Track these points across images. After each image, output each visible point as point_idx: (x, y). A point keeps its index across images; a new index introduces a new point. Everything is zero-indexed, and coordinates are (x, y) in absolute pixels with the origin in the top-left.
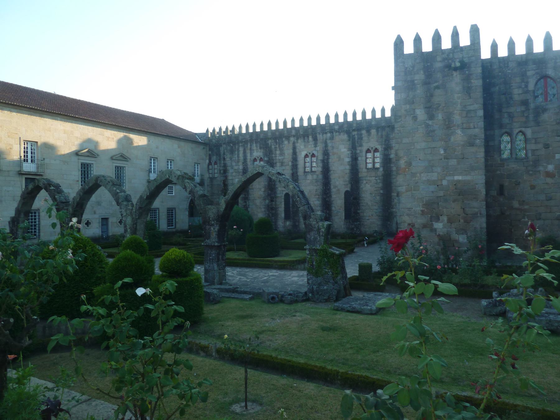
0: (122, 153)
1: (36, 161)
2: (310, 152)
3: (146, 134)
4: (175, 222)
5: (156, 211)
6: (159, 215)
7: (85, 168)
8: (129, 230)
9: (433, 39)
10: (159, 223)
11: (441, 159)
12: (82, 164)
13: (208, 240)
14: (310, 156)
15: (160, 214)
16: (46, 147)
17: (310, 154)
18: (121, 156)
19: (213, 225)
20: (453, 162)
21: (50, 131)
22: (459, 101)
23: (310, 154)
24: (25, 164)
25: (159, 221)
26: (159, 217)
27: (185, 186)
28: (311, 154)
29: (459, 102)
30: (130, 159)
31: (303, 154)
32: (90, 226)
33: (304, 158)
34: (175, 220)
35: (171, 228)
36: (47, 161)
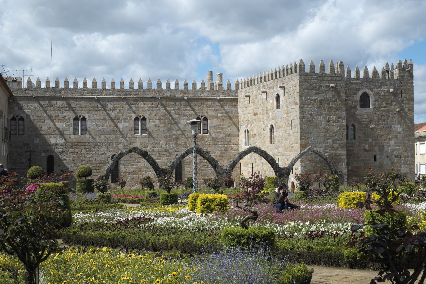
2: (140, 115)
3: (7, 89)
20: (331, 141)
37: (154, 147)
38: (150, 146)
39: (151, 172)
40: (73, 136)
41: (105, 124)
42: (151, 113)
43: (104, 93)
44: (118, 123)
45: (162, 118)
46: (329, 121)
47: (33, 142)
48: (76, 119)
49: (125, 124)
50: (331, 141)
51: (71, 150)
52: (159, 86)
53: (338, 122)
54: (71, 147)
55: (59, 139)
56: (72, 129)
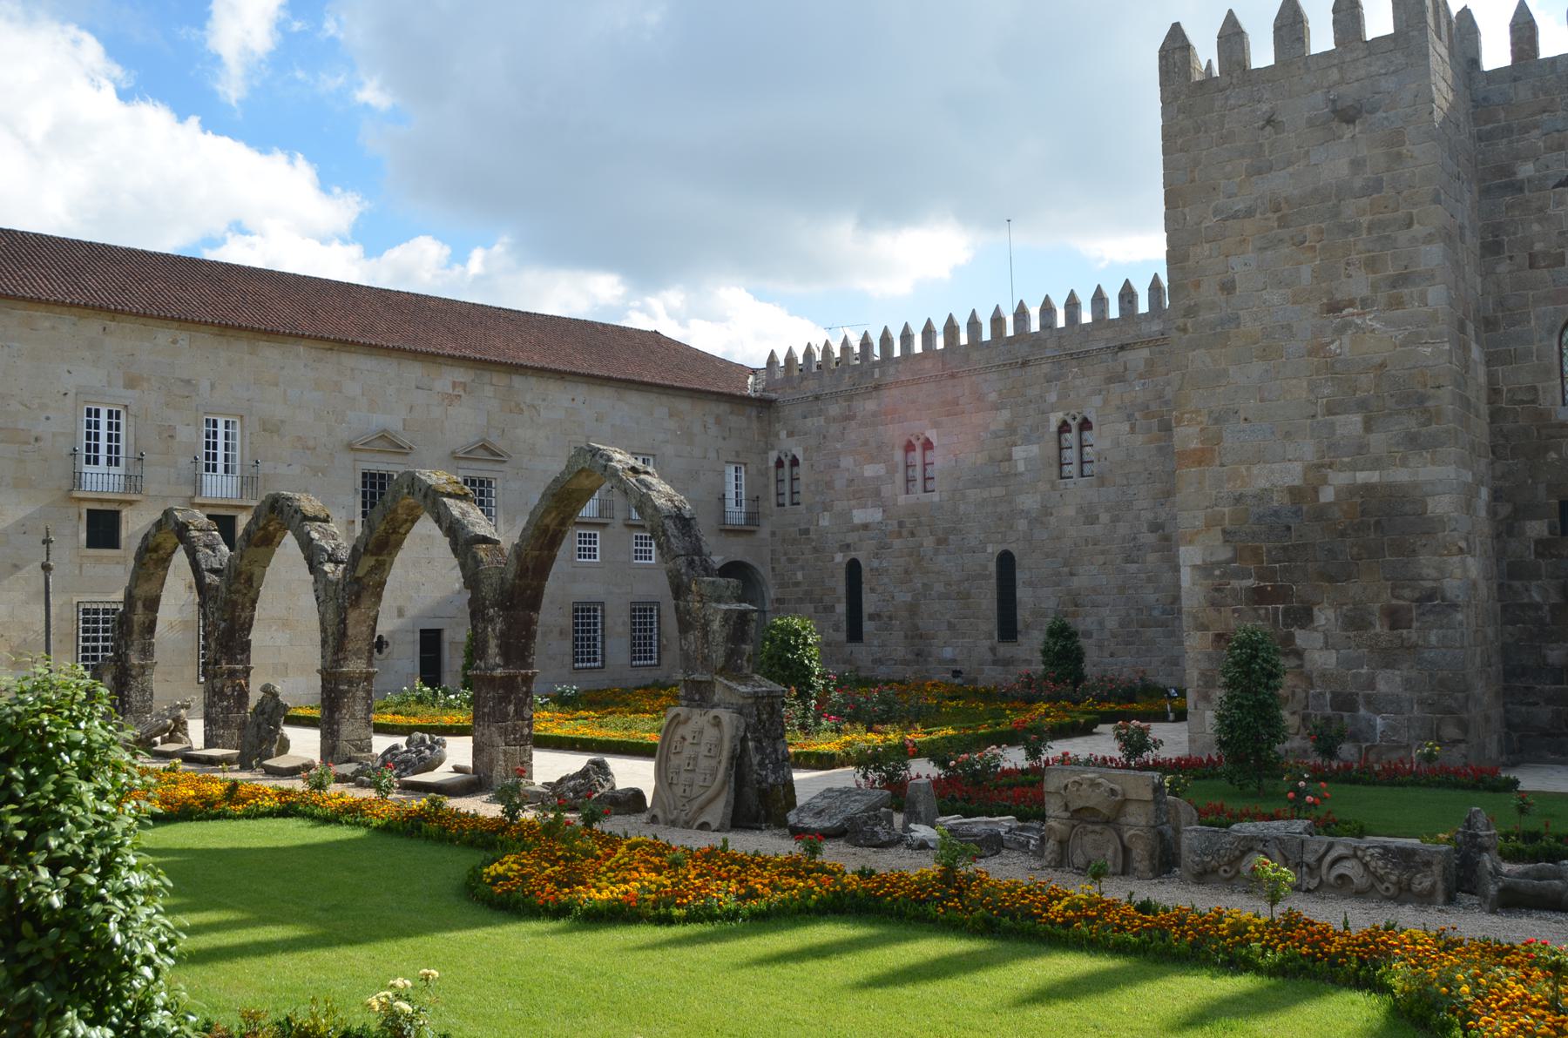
0: (484, 440)
1: (238, 469)
2: (1073, 412)
4: (659, 647)
5: (595, 610)
6: (603, 623)
7: (373, 485)
8: (331, 639)
9: (1278, 29)
10: (603, 649)
11: (1313, 416)
12: (364, 475)
13: (481, 660)
14: (1074, 424)
15: (608, 621)
16: (264, 430)
17: (1074, 419)
18: (483, 447)
19: (491, 620)
20: (1351, 424)
21: (276, 385)
22: (1365, 220)
23: (1074, 419)
24: (208, 478)
25: (603, 642)
26: (603, 630)
27: (438, 513)
28: (1079, 419)
29: (1365, 225)
30: (510, 456)
31: (1055, 419)
32: (386, 651)
33: (1055, 436)
34: (659, 641)
35: (647, 666)
36: (265, 468)
37: (1115, 520)
38: (1104, 518)
39: (1108, 605)
40: (902, 499)
41: (979, 456)
42: (1106, 402)
43: (975, 356)
44: (1012, 446)
45: (1137, 415)
46: (1334, 308)
47: (817, 525)
48: (909, 447)
49: (1030, 447)
50: (1351, 424)
51: (897, 543)
52: (1127, 305)
53: (1396, 303)
54: (900, 535)
55: (870, 511)
56: (899, 478)
